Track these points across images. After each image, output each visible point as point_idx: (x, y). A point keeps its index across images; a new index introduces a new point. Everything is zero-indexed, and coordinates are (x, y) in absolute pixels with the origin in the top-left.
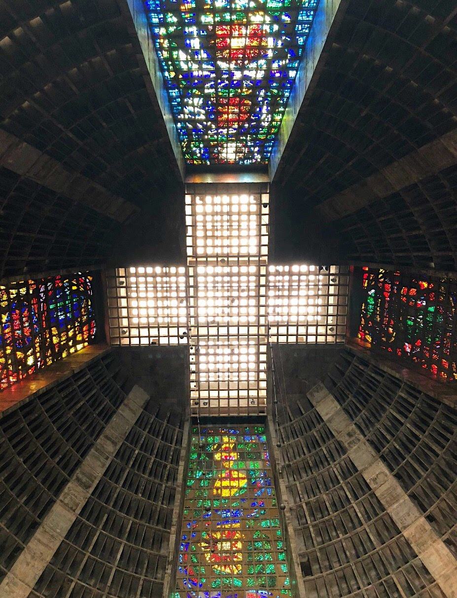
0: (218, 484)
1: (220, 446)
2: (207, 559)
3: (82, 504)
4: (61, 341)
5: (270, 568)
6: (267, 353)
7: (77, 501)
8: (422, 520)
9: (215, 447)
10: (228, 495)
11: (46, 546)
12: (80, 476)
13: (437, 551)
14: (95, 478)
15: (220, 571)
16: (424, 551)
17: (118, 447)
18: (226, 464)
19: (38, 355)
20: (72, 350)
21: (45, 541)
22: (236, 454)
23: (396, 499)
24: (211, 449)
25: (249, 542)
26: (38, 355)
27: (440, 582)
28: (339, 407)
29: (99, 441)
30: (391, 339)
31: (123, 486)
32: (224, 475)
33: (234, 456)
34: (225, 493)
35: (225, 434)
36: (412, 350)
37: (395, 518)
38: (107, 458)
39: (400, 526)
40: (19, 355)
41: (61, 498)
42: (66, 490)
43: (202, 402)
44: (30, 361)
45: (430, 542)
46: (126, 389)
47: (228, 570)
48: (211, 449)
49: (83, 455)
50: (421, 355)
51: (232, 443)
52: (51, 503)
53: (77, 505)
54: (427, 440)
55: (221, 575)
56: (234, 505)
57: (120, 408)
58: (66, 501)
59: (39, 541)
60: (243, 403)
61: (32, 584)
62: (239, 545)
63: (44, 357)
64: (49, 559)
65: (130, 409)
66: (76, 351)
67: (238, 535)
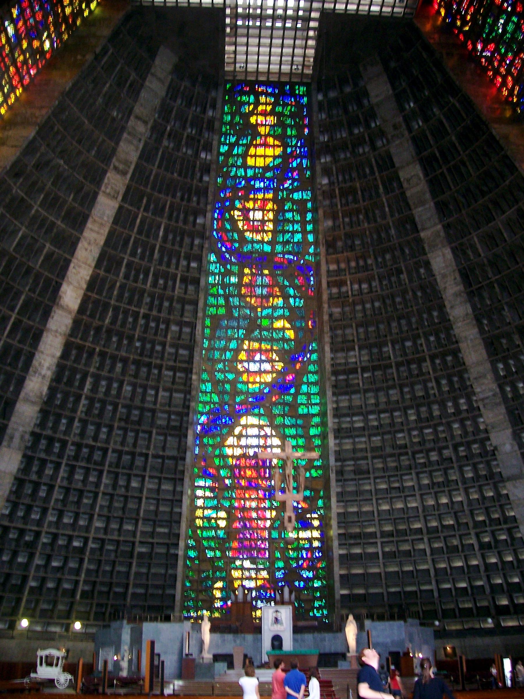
0: (252, 151)
1: (256, 107)
2: (240, 227)
3: (122, 190)
4: (73, 10)
5: (298, 237)
6: (320, 20)
7: (117, 189)
8: (439, 227)
9: (251, 109)
10: (262, 165)
11: (98, 233)
12: (117, 164)
13: (444, 255)
14: (131, 163)
15: (253, 238)
16: (433, 252)
17: (149, 126)
18: (262, 130)
19: (53, 36)
20: (86, 14)
21: (96, 229)
22: (272, 118)
23: (422, 203)
24: (246, 109)
25: (280, 211)
26: (53, 36)
27: (439, 278)
28: (391, 92)
29: (130, 123)
30: (465, 26)
31: (159, 167)
32: (258, 142)
33: (271, 120)
34: (260, 162)
35: (262, 93)
36: (483, 50)
37: (417, 219)
38: (140, 140)
39: (419, 227)
40: (36, 44)
41: (103, 188)
42: (106, 181)
43: (238, 65)
44: (47, 45)
45: (440, 246)
46: (153, 54)
47: (259, 237)
48: (246, 109)
49: (117, 143)
50: (489, 60)
51: (269, 104)
52: (95, 195)
53: (118, 193)
54: (465, 159)
55: (252, 242)
56: (268, 175)
57: (148, 79)
58: (108, 191)
59: (91, 230)
60: (286, 68)
61: (93, 264)
62: (271, 215)
63: (59, 35)
64: (102, 243)
65: (160, 80)
66: (91, 12)
67: (270, 206)
